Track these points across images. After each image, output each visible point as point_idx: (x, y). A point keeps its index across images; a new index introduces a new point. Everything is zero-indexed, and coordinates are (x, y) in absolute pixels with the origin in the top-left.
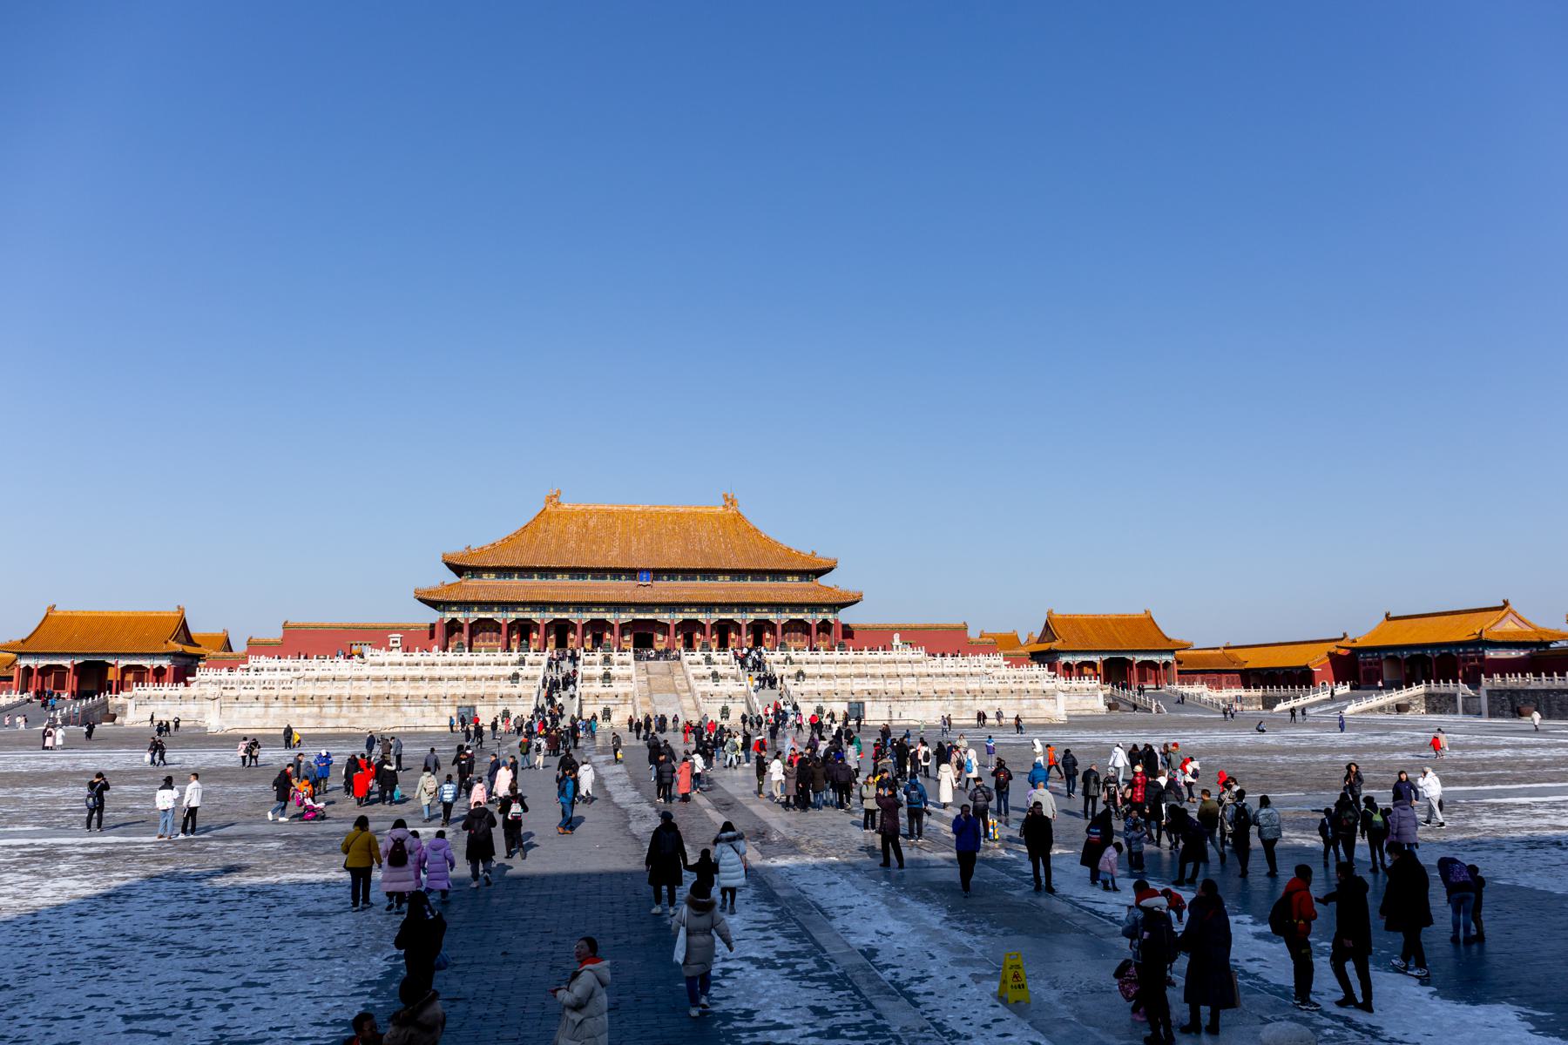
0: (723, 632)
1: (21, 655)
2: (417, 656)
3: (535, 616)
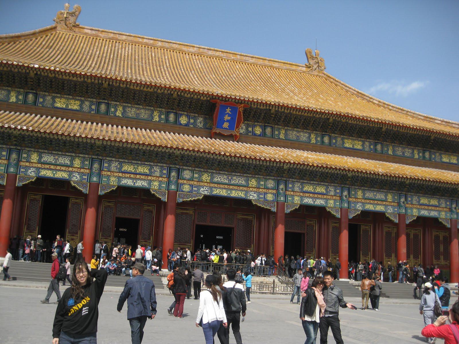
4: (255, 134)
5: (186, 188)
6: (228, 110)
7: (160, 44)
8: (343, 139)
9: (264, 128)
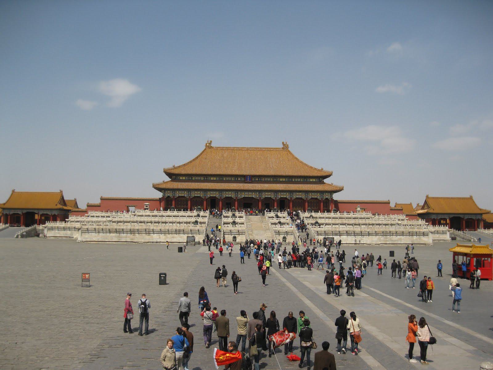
0: (282, 205)
2: (156, 213)
4: (256, 181)
5: (239, 196)
6: (248, 177)
7: (235, 149)
8: (280, 179)
9: (258, 179)
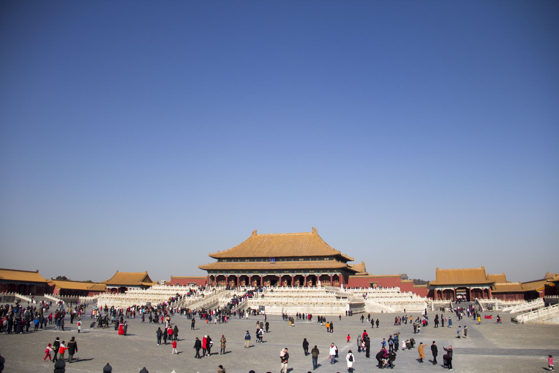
1: (108, 285)
3: (277, 275)
